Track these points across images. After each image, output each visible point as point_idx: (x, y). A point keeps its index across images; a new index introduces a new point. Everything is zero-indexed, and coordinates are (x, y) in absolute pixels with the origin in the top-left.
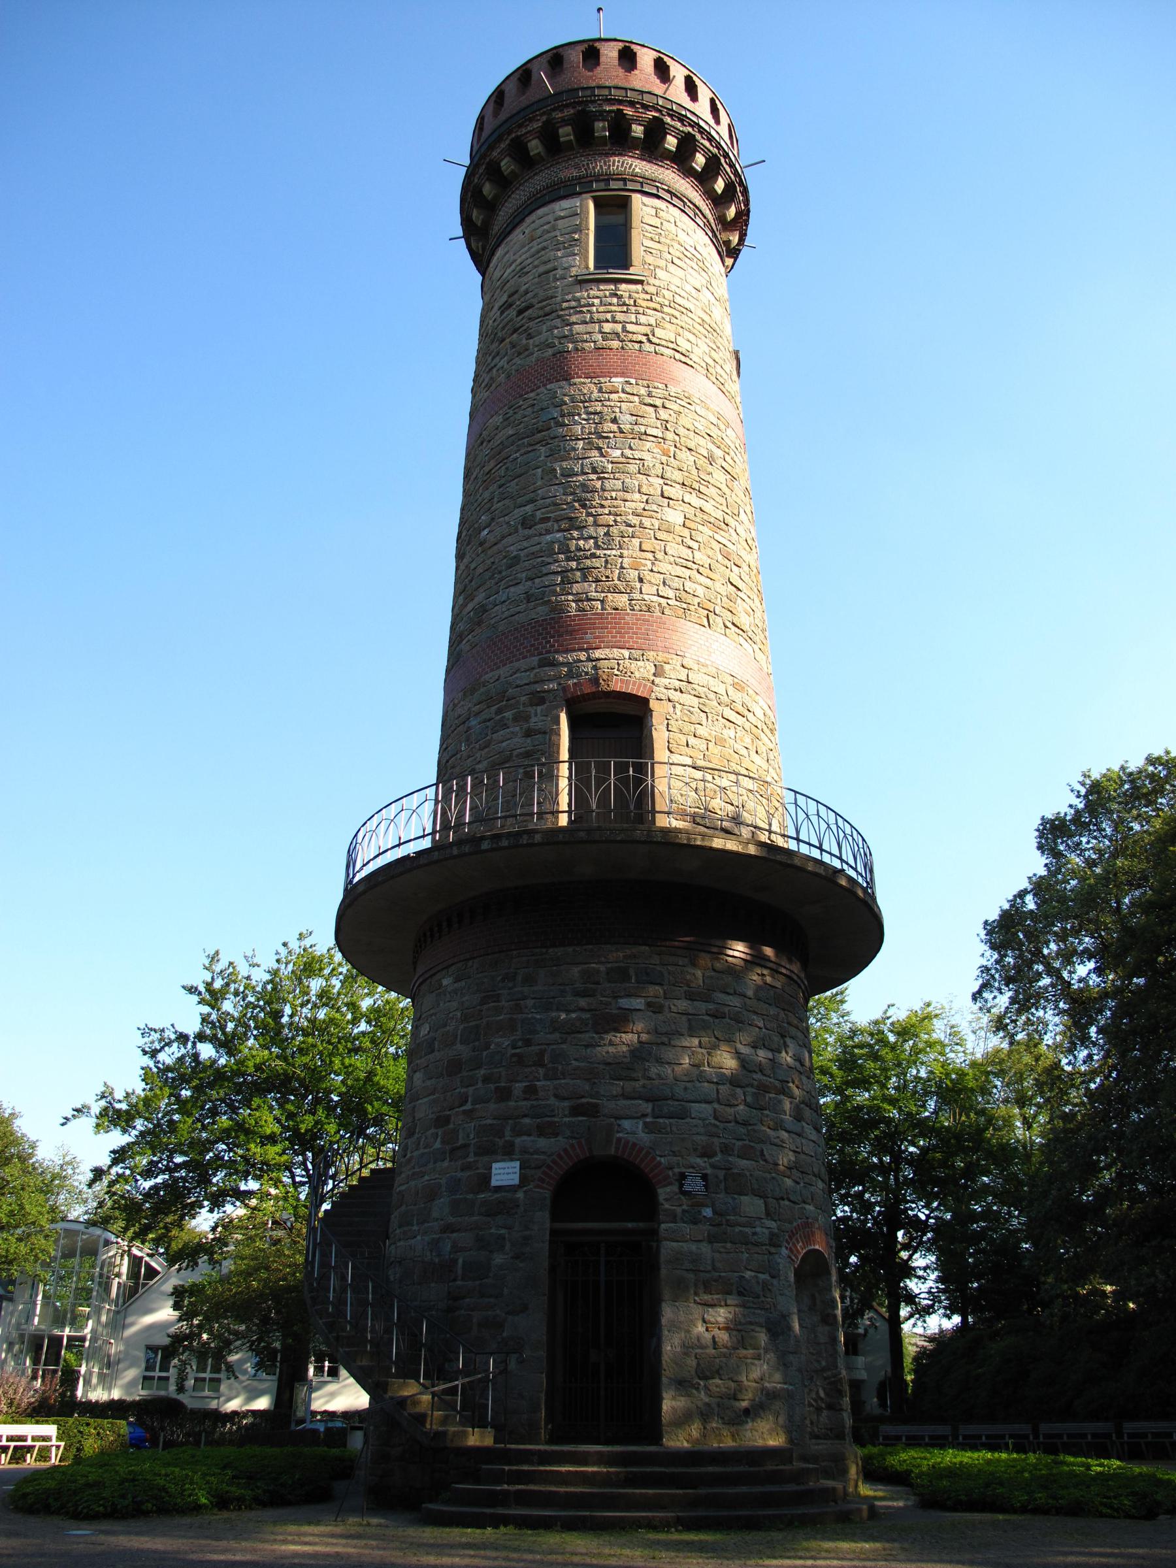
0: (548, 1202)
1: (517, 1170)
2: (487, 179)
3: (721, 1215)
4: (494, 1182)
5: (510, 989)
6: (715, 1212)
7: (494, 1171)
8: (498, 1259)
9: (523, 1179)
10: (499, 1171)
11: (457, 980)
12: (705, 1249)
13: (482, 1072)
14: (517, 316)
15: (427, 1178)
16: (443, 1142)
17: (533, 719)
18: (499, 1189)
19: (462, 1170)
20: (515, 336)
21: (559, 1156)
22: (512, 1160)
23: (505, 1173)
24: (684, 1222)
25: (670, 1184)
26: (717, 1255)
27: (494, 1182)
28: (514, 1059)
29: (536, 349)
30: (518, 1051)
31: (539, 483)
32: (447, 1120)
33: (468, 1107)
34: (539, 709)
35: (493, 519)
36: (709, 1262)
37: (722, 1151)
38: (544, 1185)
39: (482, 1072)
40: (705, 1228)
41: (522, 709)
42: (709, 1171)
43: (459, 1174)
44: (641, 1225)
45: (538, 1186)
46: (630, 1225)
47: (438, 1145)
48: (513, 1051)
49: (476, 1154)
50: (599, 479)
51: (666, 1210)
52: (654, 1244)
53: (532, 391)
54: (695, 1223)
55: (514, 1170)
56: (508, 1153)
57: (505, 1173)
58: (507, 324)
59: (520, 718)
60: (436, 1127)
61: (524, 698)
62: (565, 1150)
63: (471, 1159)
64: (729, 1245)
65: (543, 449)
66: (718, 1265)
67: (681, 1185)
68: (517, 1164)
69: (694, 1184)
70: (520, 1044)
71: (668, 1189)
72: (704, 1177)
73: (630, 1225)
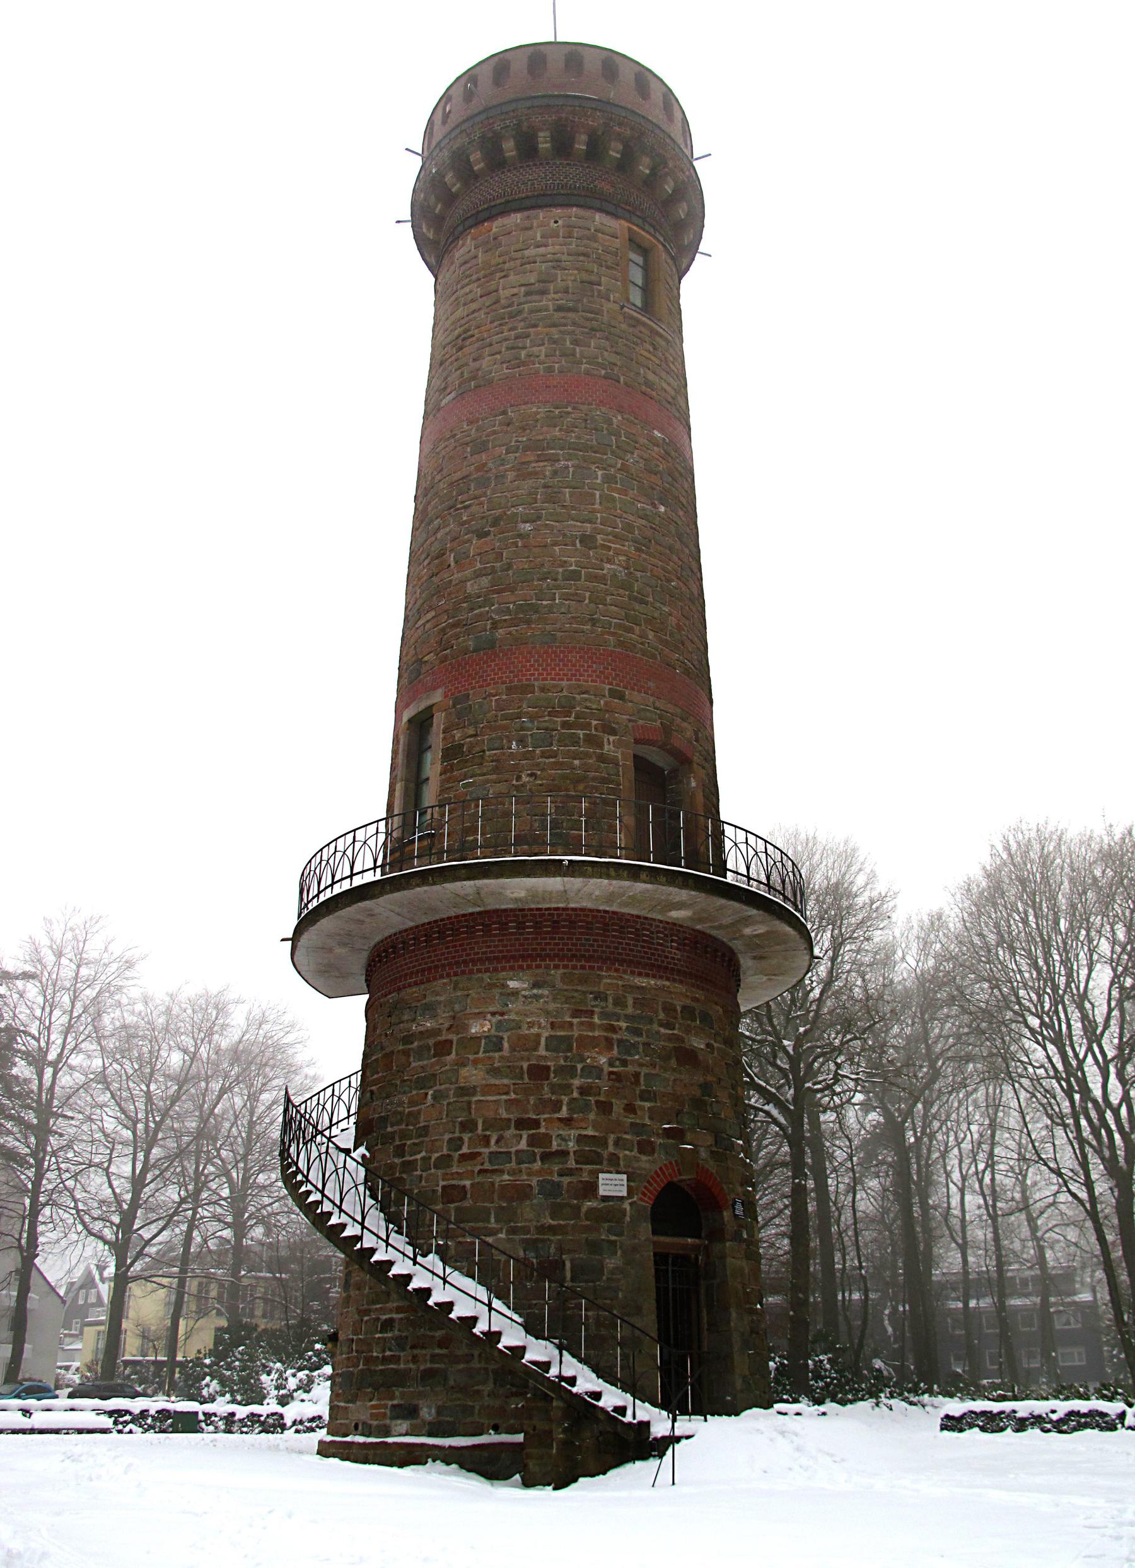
1: (625, 1182)
2: (514, 137)
4: (602, 1191)
5: (602, 1008)
7: (601, 1181)
8: (611, 1263)
9: (630, 1190)
10: (604, 1182)
11: (535, 985)
13: (576, 1082)
14: (555, 310)
15: (506, 1177)
16: (530, 1143)
17: (606, 747)
18: (606, 1198)
19: (561, 1175)
20: (553, 330)
21: (656, 1172)
22: (618, 1172)
23: (612, 1185)
27: (602, 1191)
28: (613, 1077)
29: (584, 361)
30: (615, 1070)
31: (597, 506)
32: (536, 1124)
33: (564, 1112)
34: (612, 738)
35: (539, 518)
38: (646, 1199)
39: (576, 1082)
41: (593, 732)
43: (556, 1178)
45: (641, 1199)
47: (523, 1145)
48: (611, 1069)
49: (577, 1162)
50: (651, 528)
53: (583, 404)
55: (621, 1183)
56: (614, 1165)
57: (612, 1185)
58: (540, 311)
59: (591, 740)
60: (517, 1128)
61: (596, 722)
62: (661, 1169)
63: (572, 1163)
65: (600, 473)
68: (625, 1177)
70: (617, 1063)
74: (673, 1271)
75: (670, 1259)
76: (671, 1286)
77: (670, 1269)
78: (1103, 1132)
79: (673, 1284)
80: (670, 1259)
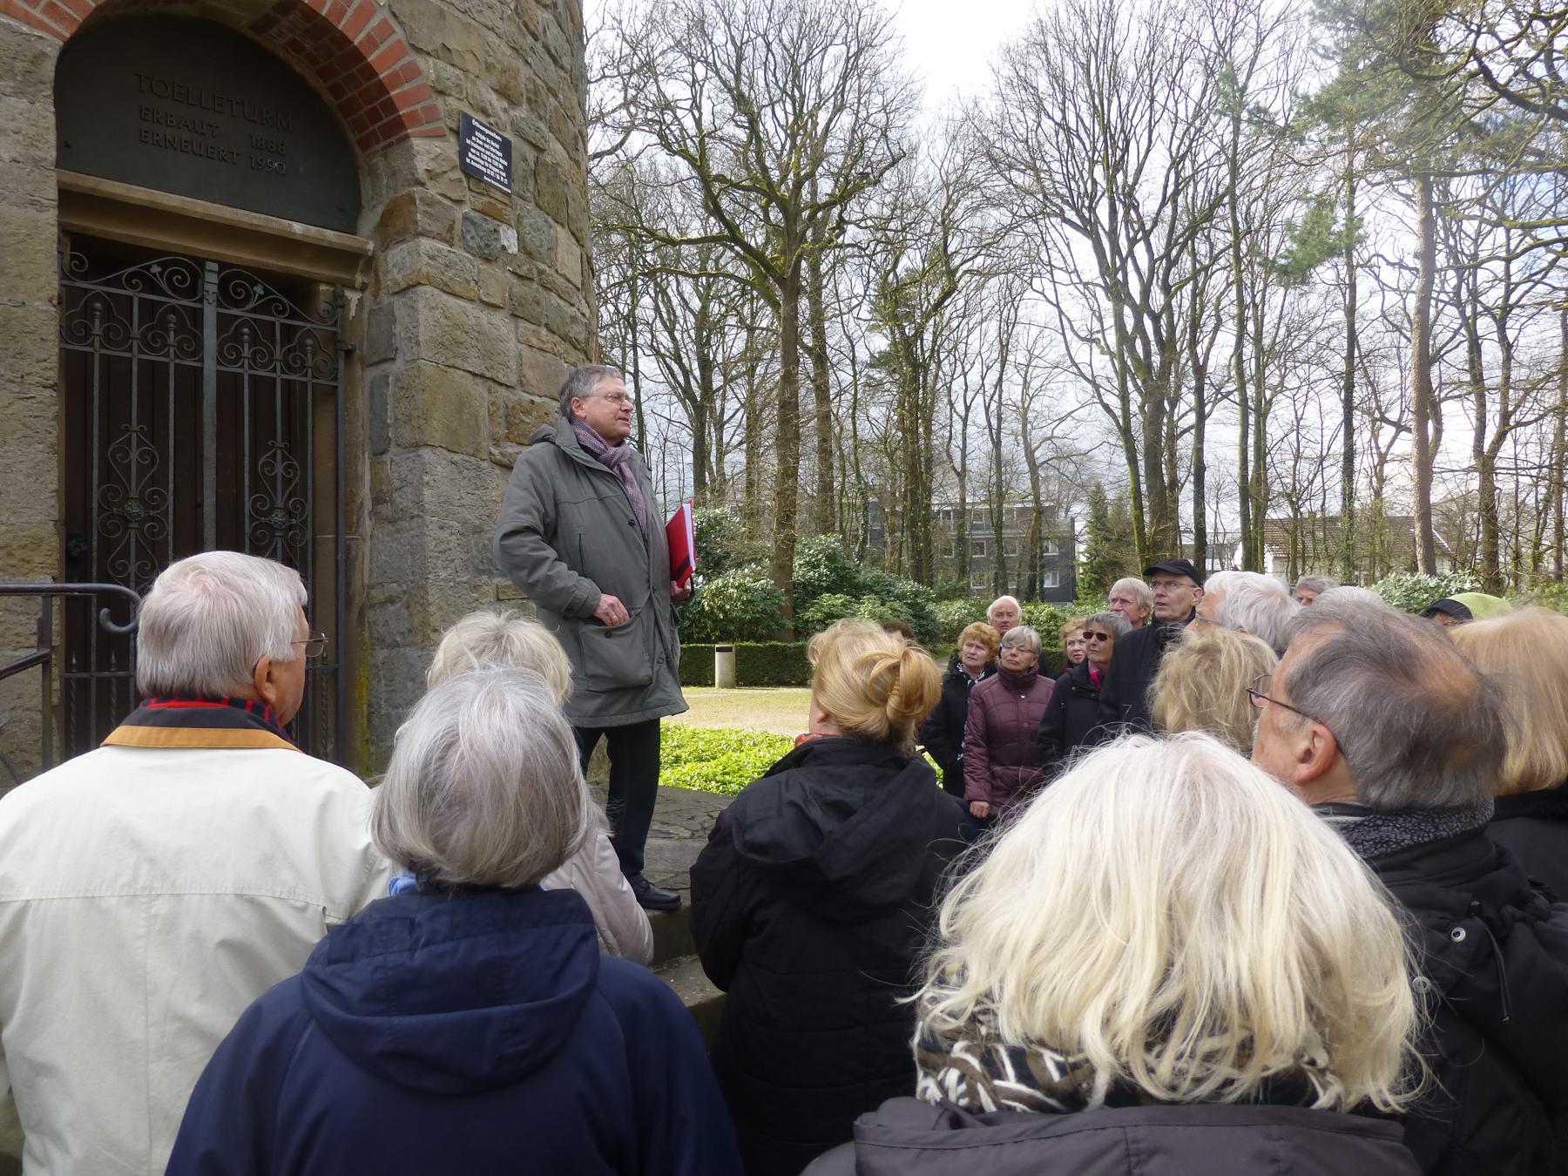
0: (48, 69)
3: (530, 254)
6: (523, 247)
12: (500, 324)
24: (468, 249)
25: (440, 136)
26: (526, 351)
36: (513, 364)
37: (529, 100)
38: (37, 13)
40: (497, 282)
42: (509, 135)
44: (331, 236)
46: (298, 228)
51: (430, 203)
52: (353, 297)
54: (487, 260)
64: (544, 331)
66: (531, 375)
67: (464, 150)
69: (486, 158)
71: (436, 146)
72: (505, 147)
73: (298, 228)
74: (223, 322)
75: (211, 279)
76: (210, 367)
77: (210, 313)
78: (1138, 344)
79: (221, 358)
80: (211, 279)
